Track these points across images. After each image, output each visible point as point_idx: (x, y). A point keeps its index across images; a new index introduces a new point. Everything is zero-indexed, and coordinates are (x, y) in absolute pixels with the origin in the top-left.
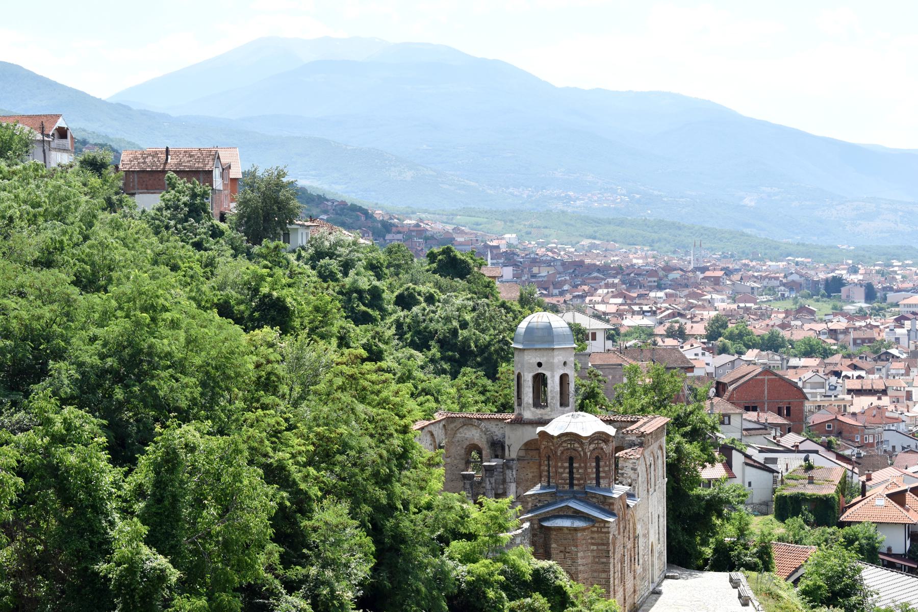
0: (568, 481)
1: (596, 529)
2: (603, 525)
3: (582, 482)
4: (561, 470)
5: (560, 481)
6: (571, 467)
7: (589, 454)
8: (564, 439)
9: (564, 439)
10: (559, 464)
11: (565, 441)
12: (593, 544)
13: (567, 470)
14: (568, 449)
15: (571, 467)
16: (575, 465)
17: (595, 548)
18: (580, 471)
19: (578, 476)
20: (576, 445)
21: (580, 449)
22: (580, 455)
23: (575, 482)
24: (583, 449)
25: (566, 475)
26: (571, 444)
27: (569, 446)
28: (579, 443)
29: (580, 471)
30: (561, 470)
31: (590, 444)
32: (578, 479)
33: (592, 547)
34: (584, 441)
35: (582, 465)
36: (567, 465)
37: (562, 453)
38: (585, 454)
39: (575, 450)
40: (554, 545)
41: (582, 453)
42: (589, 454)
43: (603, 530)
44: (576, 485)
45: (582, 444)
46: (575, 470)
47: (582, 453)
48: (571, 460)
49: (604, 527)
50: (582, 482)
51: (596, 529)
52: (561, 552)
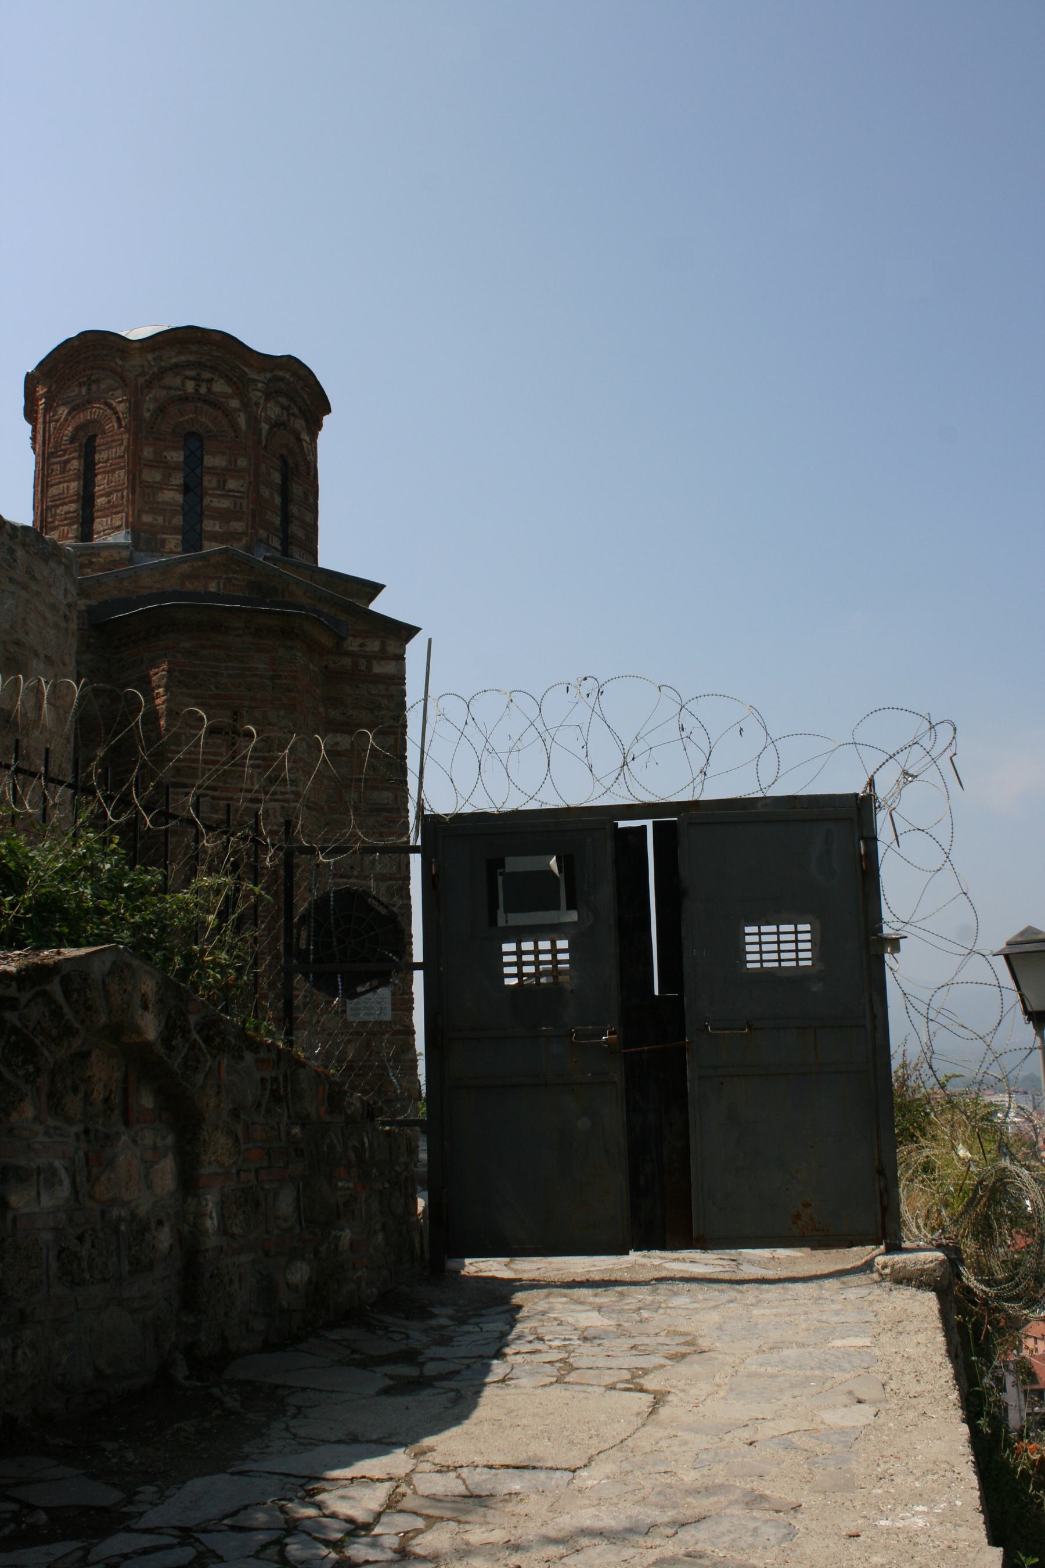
0: (178, 520)
1: (347, 662)
2: (374, 646)
6: (193, 466)
7: (265, 427)
8: (173, 357)
9: (173, 357)
10: (147, 453)
13: (178, 479)
14: (185, 399)
15: (193, 466)
16: (209, 461)
18: (232, 484)
19: (225, 504)
20: (220, 387)
21: (235, 403)
22: (234, 425)
23: (211, 526)
24: (245, 405)
25: (172, 496)
26: (197, 379)
27: (190, 386)
28: (229, 381)
29: (232, 484)
30: (151, 476)
32: (224, 516)
35: (242, 463)
36: (176, 456)
37: (161, 410)
38: (254, 421)
39: (213, 402)
41: (242, 420)
42: (265, 427)
43: (378, 669)
44: (215, 537)
46: (209, 482)
47: (242, 420)
49: (383, 656)
50: (238, 526)
51: (347, 662)
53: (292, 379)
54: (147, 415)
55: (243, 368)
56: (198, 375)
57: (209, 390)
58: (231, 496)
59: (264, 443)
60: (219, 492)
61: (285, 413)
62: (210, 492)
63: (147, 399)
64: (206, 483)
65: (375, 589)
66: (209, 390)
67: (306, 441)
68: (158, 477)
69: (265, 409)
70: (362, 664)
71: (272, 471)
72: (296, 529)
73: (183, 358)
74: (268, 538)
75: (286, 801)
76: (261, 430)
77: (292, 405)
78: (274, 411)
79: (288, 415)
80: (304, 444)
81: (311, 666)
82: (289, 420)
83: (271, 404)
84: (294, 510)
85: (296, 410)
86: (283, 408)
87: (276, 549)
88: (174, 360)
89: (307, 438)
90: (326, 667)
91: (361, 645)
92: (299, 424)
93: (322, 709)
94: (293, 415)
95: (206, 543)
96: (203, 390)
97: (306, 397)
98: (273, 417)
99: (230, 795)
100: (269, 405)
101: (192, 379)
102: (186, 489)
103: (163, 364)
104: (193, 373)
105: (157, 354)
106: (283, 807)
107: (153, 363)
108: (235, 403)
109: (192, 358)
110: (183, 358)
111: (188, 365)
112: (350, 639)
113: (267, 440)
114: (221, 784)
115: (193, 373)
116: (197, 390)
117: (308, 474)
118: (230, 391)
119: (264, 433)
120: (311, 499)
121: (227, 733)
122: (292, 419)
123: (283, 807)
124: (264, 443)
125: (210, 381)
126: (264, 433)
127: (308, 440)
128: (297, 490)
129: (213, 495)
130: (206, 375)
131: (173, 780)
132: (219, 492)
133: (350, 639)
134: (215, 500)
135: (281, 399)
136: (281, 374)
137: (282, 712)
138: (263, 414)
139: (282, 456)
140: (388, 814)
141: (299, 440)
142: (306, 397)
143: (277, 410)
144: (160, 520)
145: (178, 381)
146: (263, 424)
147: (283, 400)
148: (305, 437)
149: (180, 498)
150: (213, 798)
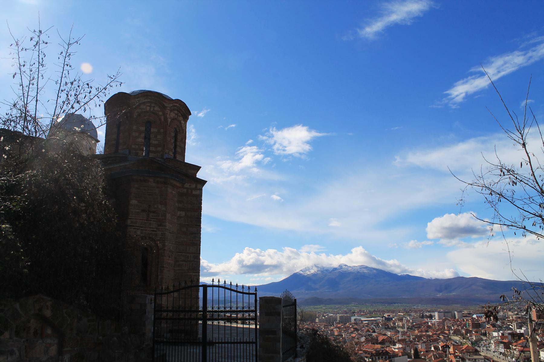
2: (194, 186)
3: (159, 149)
4: (134, 134)
5: (133, 146)
7: (169, 120)
10: (134, 127)
11: (144, 103)
12: (180, 209)
13: (143, 135)
16: (153, 130)
17: (183, 214)
18: (159, 137)
19: (156, 142)
20: (156, 108)
21: (161, 113)
26: (150, 106)
27: (148, 108)
29: (159, 137)
31: (171, 111)
33: (179, 213)
34: (166, 105)
35: (162, 130)
36: (143, 129)
38: (166, 119)
40: (134, 202)
41: (162, 118)
42: (169, 120)
43: (194, 193)
45: (163, 108)
47: (162, 118)
48: (149, 124)
49: (196, 189)
51: (185, 190)
52: (143, 211)
53: (179, 106)
54: (135, 117)
55: (164, 103)
56: (151, 105)
57: (154, 109)
58: (157, 140)
59: (169, 125)
60: (154, 139)
61: (176, 116)
62: (152, 139)
63: (135, 112)
64: (151, 136)
65: (198, 168)
66: (154, 109)
67: (183, 123)
68: (137, 134)
69: (170, 115)
70: (190, 191)
71: (171, 132)
72: (178, 149)
73: (146, 100)
74: (169, 153)
75: (162, 231)
76: (168, 121)
77: (179, 113)
78: (173, 115)
79: (177, 116)
80: (182, 124)
81: (173, 192)
82: (178, 117)
83: (172, 113)
84: (178, 143)
85: (180, 115)
86: (176, 114)
87: (172, 155)
88: (144, 101)
89: (183, 122)
90: (179, 192)
91: (190, 186)
92: (181, 118)
93: (177, 204)
94: (179, 116)
95: (150, 154)
96: (152, 109)
97: (183, 110)
98: (172, 117)
99: (146, 229)
100: (171, 114)
101: (148, 106)
102: (145, 138)
103: (140, 102)
104: (149, 105)
105: (139, 99)
106: (162, 233)
107: (137, 102)
108: (161, 113)
109: (149, 100)
110: (146, 100)
111: (148, 102)
112: (186, 184)
113: (170, 123)
114: (144, 226)
115: (149, 105)
116: (150, 109)
117: (183, 132)
118: (160, 110)
119: (169, 122)
120: (184, 140)
121: (147, 211)
122: (178, 117)
123: (162, 233)
124: (169, 125)
125: (154, 107)
126: (169, 122)
127: (184, 123)
128: (179, 138)
129: (152, 140)
130: (153, 105)
131: (130, 224)
132: (154, 139)
133: (186, 184)
134: (153, 141)
135: (175, 112)
136: (175, 104)
137: (163, 206)
138: (169, 116)
139: (175, 128)
140: (195, 235)
141: (181, 123)
142: (183, 110)
143: (174, 115)
144: (137, 147)
145: (145, 107)
146: (169, 119)
147: (176, 112)
148: (182, 122)
149: (143, 140)
150: (142, 230)
